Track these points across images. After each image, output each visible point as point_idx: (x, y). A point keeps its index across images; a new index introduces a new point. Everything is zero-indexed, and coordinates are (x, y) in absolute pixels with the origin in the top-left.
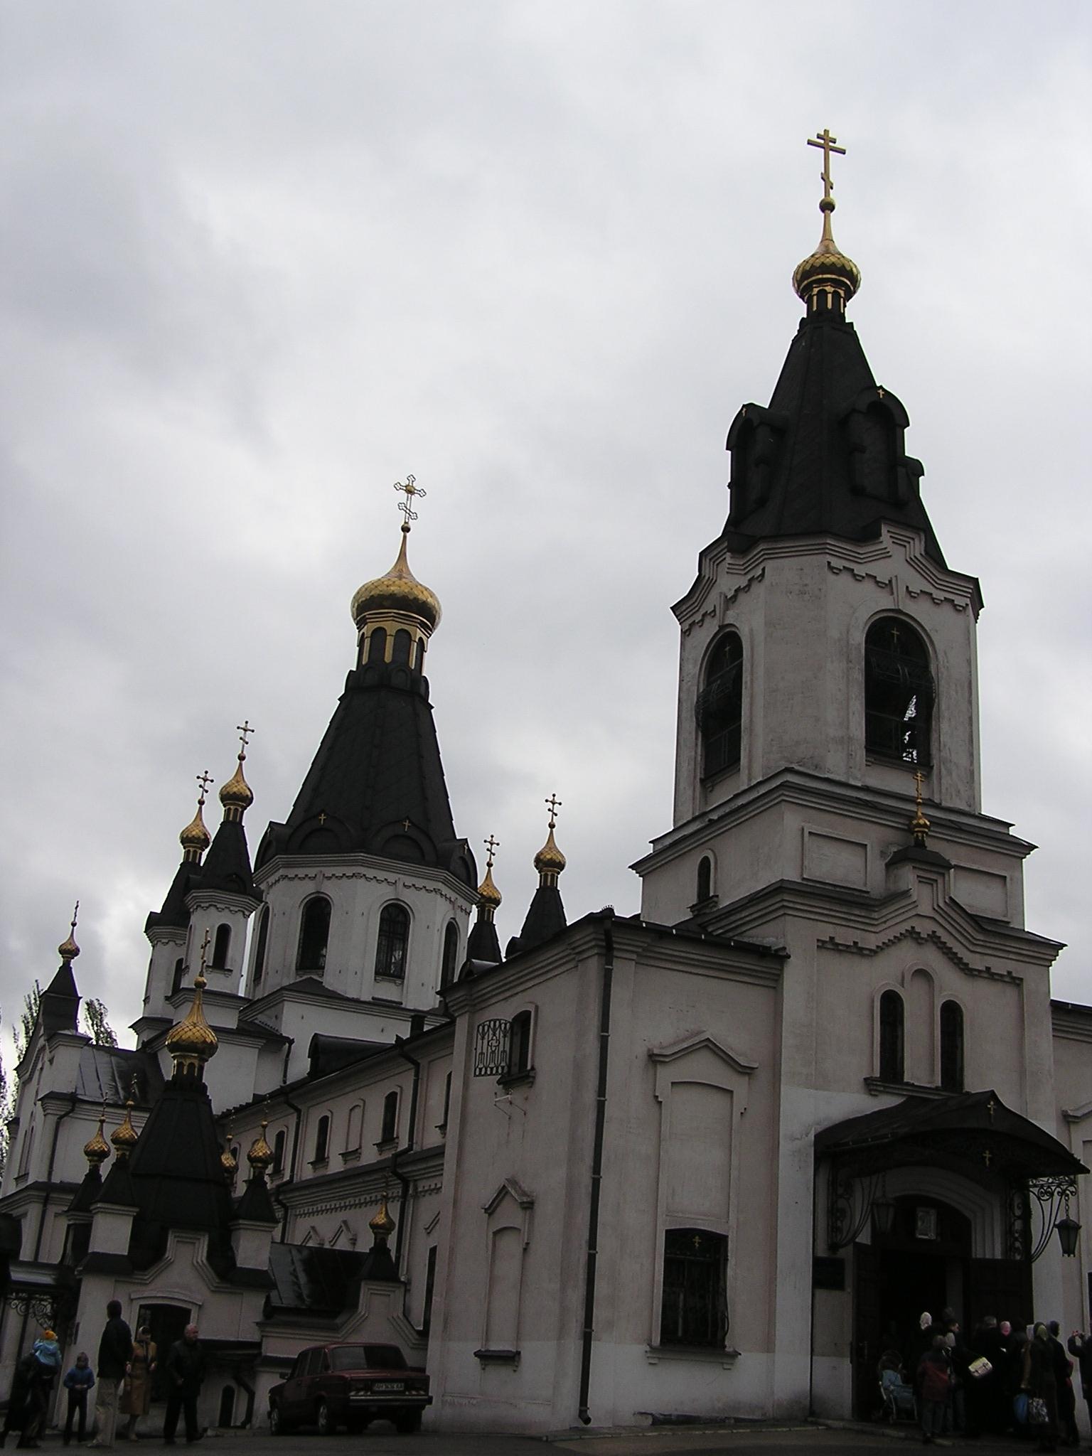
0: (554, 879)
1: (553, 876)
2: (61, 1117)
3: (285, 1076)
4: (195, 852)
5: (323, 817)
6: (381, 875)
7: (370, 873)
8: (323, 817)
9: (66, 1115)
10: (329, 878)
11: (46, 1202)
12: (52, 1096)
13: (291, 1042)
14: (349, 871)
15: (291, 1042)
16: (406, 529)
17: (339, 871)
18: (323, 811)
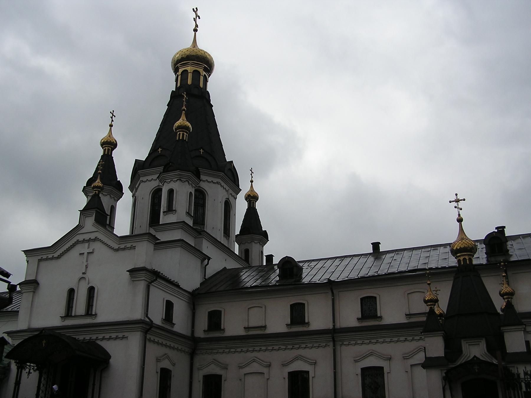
0: (254, 204)
1: (253, 203)
2: (150, 283)
3: (205, 276)
4: (109, 149)
5: (160, 150)
6: (225, 186)
7: (223, 184)
8: (160, 150)
9: (152, 282)
10: (204, 181)
11: (146, 332)
12: (144, 269)
13: (209, 259)
14: (215, 180)
15: (209, 259)
16: (195, 30)
17: (210, 179)
18: (202, 148)
